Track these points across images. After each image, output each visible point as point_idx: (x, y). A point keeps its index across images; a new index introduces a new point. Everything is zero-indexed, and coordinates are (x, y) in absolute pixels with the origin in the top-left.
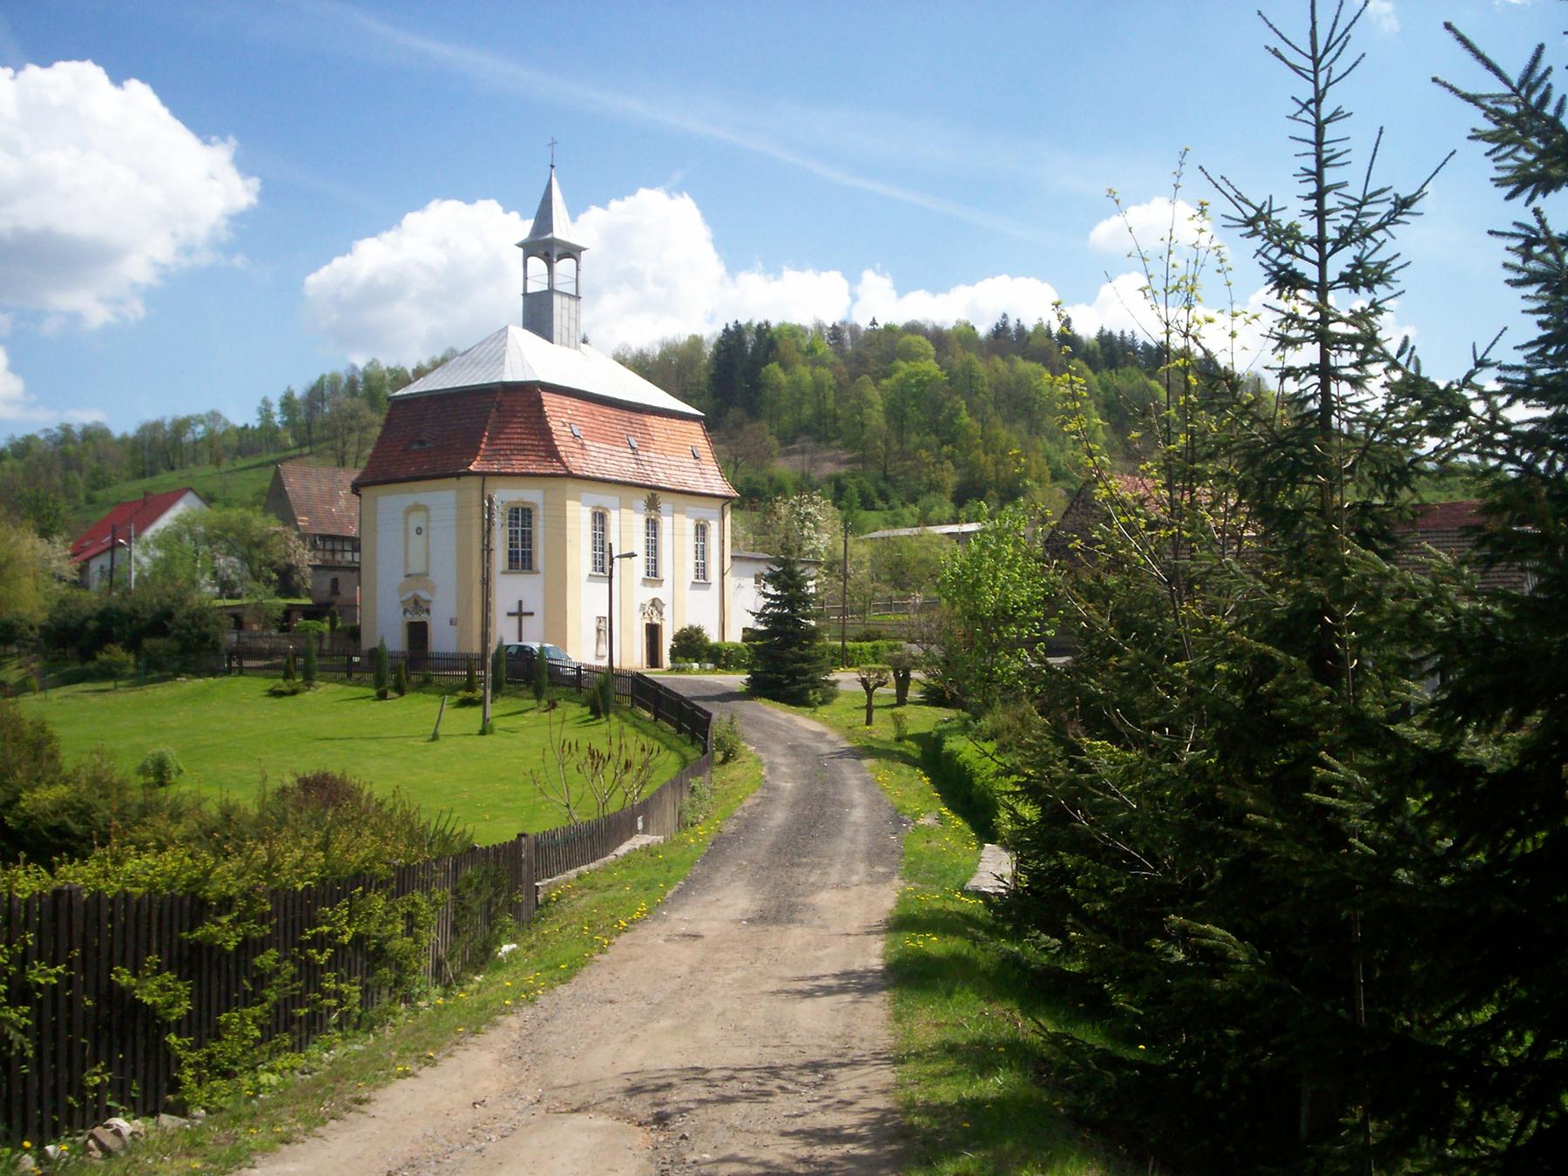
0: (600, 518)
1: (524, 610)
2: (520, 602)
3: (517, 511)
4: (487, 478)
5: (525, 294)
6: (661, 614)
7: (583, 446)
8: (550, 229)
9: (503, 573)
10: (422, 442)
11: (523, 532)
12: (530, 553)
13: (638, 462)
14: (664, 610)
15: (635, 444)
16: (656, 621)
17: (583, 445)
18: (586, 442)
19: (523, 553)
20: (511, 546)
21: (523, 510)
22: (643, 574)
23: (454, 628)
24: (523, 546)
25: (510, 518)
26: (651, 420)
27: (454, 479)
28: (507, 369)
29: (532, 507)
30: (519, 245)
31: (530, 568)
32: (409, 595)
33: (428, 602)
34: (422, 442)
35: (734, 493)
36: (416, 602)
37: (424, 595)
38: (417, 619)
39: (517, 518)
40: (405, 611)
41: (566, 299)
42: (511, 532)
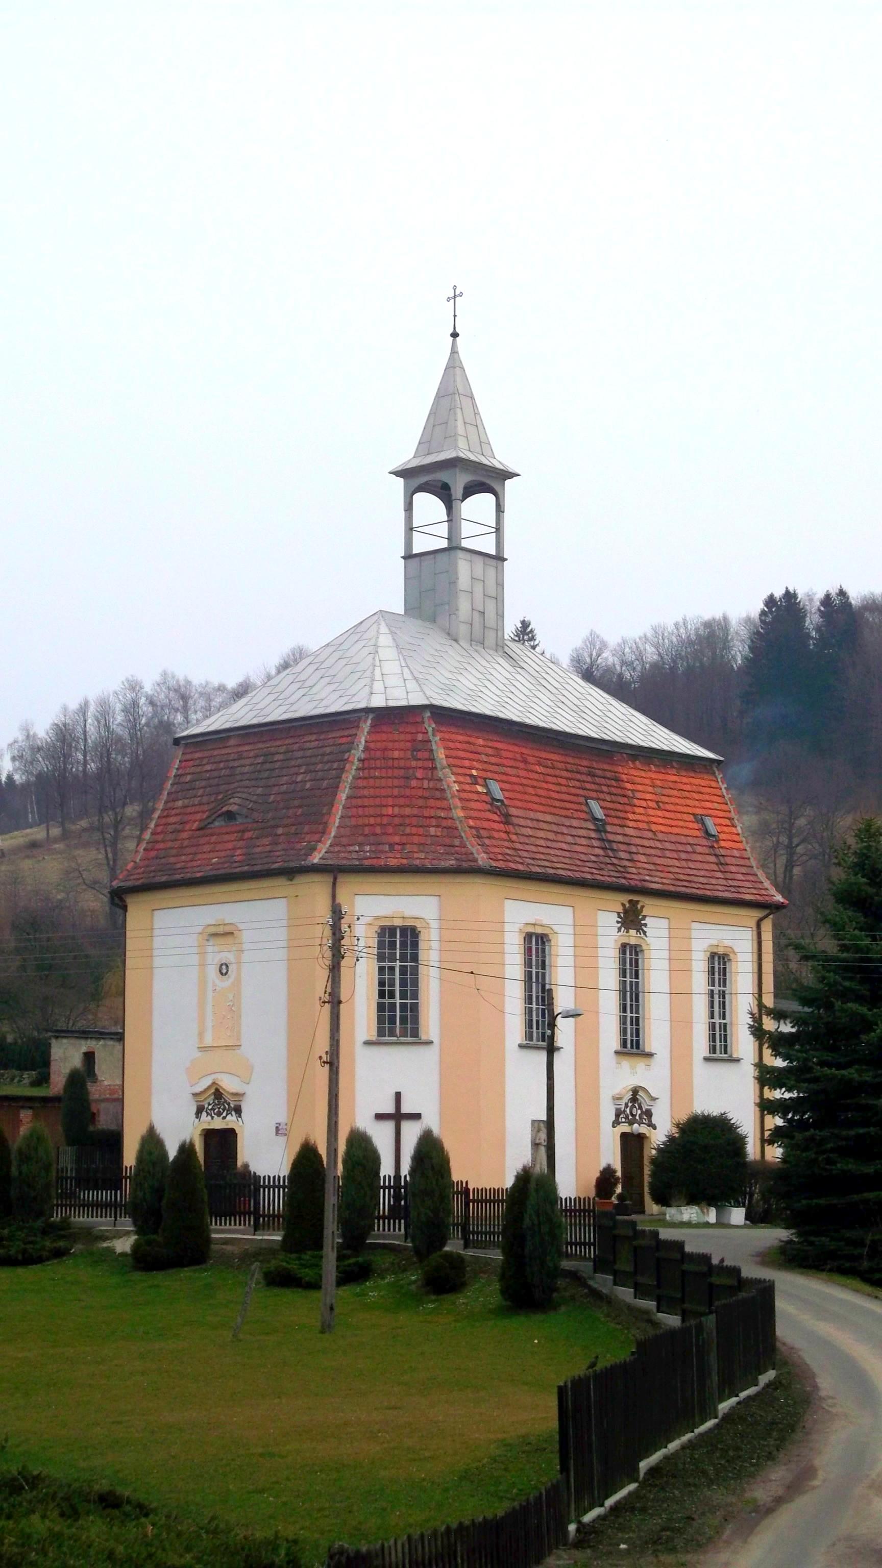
1: (405, 1109)
2: (398, 1095)
3: (392, 930)
4: (341, 879)
5: (409, 557)
6: (649, 1114)
7: (507, 819)
8: (451, 438)
9: (368, 1043)
10: (230, 815)
11: (403, 971)
12: (415, 1008)
13: (607, 845)
15: (599, 813)
17: (507, 815)
18: (513, 811)
19: (404, 1007)
20: (381, 994)
21: (404, 930)
22: (616, 1044)
23: (282, 1140)
24: (403, 996)
25: (381, 945)
27: (281, 881)
28: (378, 686)
29: (418, 924)
30: (398, 473)
31: (415, 1033)
32: (206, 1082)
33: (239, 1095)
36: (218, 1094)
37: (229, 1084)
38: (218, 1124)
39: (392, 945)
40: (199, 1111)
41: (479, 561)
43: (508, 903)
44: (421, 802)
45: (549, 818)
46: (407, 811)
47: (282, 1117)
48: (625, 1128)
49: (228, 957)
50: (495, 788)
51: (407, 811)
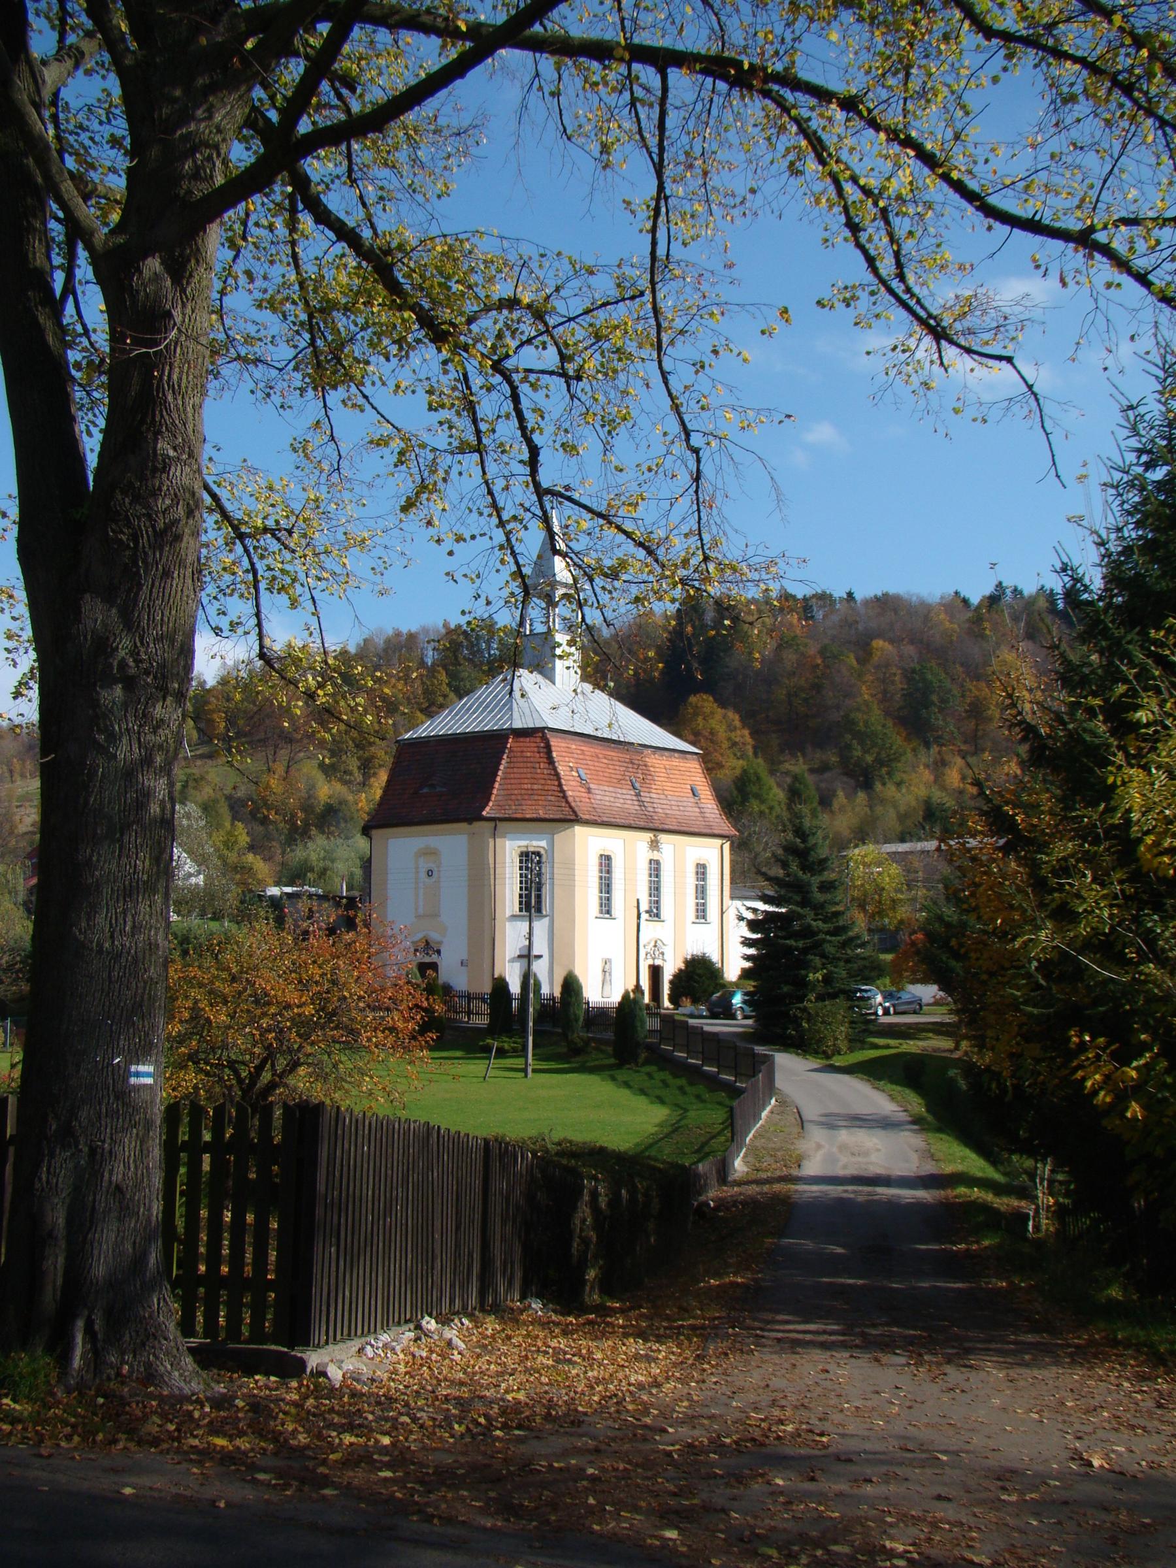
0: (606, 862)
6: (663, 954)
7: (589, 791)
14: (665, 950)
16: (658, 962)
17: (589, 789)
18: (592, 786)
26: (653, 760)
28: (516, 715)
32: (419, 936)
33: (440, 943)
34: (433, 786)
35: (734, 832)
36: (427, 943)
37: (434, 936)
42: (521, 875)
43: (590, 838)
44: (543, 782)
45: (611, 789)
46: (535, 787)
47: (465, 957)
48: (650, 962)
49: (431, 866)
50: (582, 772)
51: (535, 787)
